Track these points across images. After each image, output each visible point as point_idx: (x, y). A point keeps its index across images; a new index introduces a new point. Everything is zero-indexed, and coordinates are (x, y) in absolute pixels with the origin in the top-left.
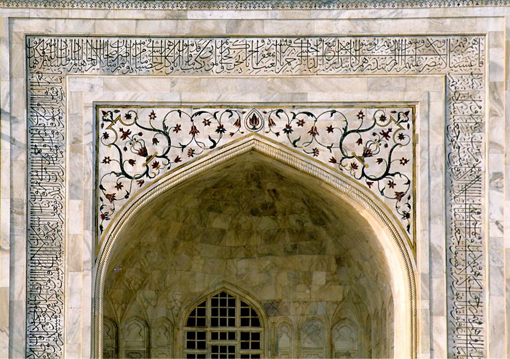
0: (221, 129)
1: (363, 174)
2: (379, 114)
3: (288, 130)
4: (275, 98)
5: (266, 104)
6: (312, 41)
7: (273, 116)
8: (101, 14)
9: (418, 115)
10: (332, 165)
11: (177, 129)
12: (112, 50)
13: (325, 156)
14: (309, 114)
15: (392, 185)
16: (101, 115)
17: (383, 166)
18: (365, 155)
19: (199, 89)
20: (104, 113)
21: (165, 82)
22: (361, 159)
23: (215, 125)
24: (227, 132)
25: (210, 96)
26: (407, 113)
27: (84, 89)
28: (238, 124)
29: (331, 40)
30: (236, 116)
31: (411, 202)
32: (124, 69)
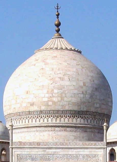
6: (69, 155)
32: (35, 160)
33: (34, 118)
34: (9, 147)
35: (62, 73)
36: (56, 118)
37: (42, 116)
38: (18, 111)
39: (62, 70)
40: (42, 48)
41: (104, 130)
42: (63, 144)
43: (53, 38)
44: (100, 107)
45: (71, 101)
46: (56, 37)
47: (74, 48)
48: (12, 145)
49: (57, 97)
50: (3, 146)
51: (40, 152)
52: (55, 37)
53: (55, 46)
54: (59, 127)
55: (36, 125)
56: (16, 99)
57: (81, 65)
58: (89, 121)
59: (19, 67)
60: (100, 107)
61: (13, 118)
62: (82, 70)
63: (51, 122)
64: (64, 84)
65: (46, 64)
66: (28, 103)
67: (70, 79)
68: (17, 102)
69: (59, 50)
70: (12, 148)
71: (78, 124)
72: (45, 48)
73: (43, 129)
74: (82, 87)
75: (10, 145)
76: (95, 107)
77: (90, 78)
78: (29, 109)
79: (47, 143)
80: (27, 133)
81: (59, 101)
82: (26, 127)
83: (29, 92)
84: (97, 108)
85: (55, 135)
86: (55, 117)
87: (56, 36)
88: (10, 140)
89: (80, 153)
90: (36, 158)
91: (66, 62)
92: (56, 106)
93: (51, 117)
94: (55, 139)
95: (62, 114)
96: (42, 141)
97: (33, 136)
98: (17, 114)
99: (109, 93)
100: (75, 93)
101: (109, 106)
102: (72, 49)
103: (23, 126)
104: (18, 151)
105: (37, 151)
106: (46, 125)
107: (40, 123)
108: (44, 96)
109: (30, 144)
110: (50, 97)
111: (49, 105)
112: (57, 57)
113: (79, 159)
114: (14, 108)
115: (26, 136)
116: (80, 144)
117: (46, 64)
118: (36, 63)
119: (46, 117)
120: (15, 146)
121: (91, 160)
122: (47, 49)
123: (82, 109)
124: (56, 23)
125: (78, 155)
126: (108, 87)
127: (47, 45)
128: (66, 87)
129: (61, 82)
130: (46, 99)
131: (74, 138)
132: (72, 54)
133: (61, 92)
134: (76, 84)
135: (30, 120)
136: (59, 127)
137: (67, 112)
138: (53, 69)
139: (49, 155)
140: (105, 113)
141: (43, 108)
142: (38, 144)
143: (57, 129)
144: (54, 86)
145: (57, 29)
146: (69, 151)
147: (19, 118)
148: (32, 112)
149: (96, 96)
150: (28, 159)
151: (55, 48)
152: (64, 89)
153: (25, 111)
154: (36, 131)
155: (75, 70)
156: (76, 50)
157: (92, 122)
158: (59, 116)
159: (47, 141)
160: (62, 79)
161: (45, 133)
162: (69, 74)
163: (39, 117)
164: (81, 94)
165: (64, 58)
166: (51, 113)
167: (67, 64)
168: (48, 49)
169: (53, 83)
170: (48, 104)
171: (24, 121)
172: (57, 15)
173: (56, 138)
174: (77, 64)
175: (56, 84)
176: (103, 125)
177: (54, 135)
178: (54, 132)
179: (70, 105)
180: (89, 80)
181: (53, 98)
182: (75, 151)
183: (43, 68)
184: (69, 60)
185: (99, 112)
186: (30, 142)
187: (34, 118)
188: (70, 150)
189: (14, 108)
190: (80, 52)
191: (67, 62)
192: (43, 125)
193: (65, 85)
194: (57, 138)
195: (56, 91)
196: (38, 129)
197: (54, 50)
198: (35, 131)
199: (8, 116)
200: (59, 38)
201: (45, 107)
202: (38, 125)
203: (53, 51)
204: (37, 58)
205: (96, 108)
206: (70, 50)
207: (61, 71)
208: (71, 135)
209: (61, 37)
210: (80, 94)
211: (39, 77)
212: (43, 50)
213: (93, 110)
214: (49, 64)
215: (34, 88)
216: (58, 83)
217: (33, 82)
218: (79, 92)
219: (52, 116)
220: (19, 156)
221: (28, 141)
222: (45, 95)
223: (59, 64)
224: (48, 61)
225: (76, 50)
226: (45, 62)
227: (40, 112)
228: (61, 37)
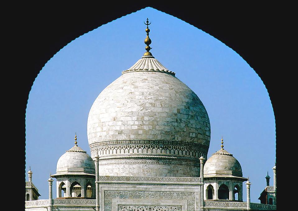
2: (175, 208)
4: (154, 204)
5: (152, 205)
6: (162, 192)
8: (119, 186)
9: (182, 208)
12: (122, 194)
14: (161, 207)
16: (119, 207)
19: (139, 201)
20: (120, 207)
21: (132, 200)
25: (142, 204)
26: (180, 208)
27: (116, 201)
28: (147, 209)
29: (165, 192)
33: (122, 148)
34: (95, 182)
35: (153, 98)
36: (147, 149)
37: (132, 146)
38: (104, 140)
39: (154, 95)
40: (130, 69)
41: (201, 164)
42: (155, 180)
43: (142, 58)
44: (197, 137)
46: (147, 56)
47: (167, 70)
48: (99, 179)
49: (148, 125)
50: (88, 180)
51: (130, 188)
52: (145, 56)
53: (146, 67)
54: (151, 159)
55: (125, 157)
56: (102, 126)
58: (184, 152)
60: (197, 137)
61: (99, 148)
62: (176, 95)
63: (141, 153)
64: (156, 111)
65: (136, 87)
66: (116, 131)
67: (162, 104)
68: (103, 130)
69: (150, 71)
70: (99, 183)
71: (171, 156)
72: (133, 69)
73: (133, 161)
74: (176, 115)
75: (96, 180)
77: (185, 104)
78: (116, 138)
79: (137, 179)
80: (115, 165)
81: (151, 130)
82: (114, 159)
83: (117, 119)
84: (194, 138)
85: (147, 168)
86: (146, 148)
87: (146, 55)
88: (96, 174)
89: (174, 190)
90: (125, 194)
91: (158, 86)
92: (147, 135)
94: (146, 172)
95: (154, 145)
96: (132, 176)
97: (122, 168)
98: (103, 144)
99: (207, 122)
100: (167, 121)
101: (207, 135)
102: (165, 71)
103: (110, 157)
104: (105, 187)
105: (127, 187)
106: (136, 156)
107: (129, 154)
108: (133, 124)
109: (119, 178)
110: (140, 125)
111: (139, 134)
112: (147, 80)
113: (173, 197)
114: (100, 136)
115: (114, 169)
116: (173, 179)
117: (135, 88)
118: (124, 86)
119: (135, 147)
120: (102, 181)
121: (186, 198)
122: (136, 70)
124: (146, 40)
125: (172, 192)
126: (206, 114)
127: (136, 66)
128: (158, 114)
129: (152, 108)
130: (136, 127)
131: (167, 172)
132: (165, 76)
133: (152, 120)
134: (169, 111)
135: (118, 151)
136: (150, 159)
138: (143, 94)
139: (139, 191)
140: (203, 144)
141: (132, 137)
142: (128, 178)
143: (148, 161)
145: (147, 47)
146: (162, 187)
147: (106, 148)
148: (120, 141)
149: (192, 125)
150: (117, 196)
151: (145, 70)
152: (156, 117)
153: (112, 140)
154: (125, 163)
155: (167, 94)
156: (169, 72)
157: (188, 154)
158: (150, 146)
159: (137, 175)
160: (153, 104)
161: (135, 165)
162: (161, 100)
163: (129, 147)
164: (175, 122)
165: (156, 81)
166: (141, 143)
167: (159, 88)
168: (137, 71)
169: (143, 109)
170: (138, 133)
171: (111, 151)
172: (146, 32)
173: (147, 171)
174: (170, 88)
175: (146, 110)
176: (199, 159)
177: (145, 168)
178: (145, 165)
179: (163, 135)
180: (183, 106)
181: (143, 126)
182: (168, 187)
184: (161, 84)
185: (195, 143)
186: (119, 176)
187: (122, 148)
188: (164, 187)
189: (100, 136)
190: (173, 74)
191: (159, 85)
192: (133, 156)
193: (156, 112)
194: (148, 171)
195: (146, 118)
196: (128, 161)
197: (143, 72)
198: (124, 163)
200: (149, 58)
201: (134, 135)
202: (127, 157)
203: (143, 73)
205: (192, 138)
206: (162, 72)
208: (164, 169)
209: (152, 56)
211: (128, 102)
212: (131, 71)
213: (188, 140)
215: (121, 114)
216: (149, 110)
218: (172, 120)
219: (142, 147)
220: (107, 192)
221: (116, 175)
222: (134, 123)
223: (149, 88)
224: (137, 84)
225: (169, 72)
226: (134, 85)
227: (129, 141)
228: (152, 56)
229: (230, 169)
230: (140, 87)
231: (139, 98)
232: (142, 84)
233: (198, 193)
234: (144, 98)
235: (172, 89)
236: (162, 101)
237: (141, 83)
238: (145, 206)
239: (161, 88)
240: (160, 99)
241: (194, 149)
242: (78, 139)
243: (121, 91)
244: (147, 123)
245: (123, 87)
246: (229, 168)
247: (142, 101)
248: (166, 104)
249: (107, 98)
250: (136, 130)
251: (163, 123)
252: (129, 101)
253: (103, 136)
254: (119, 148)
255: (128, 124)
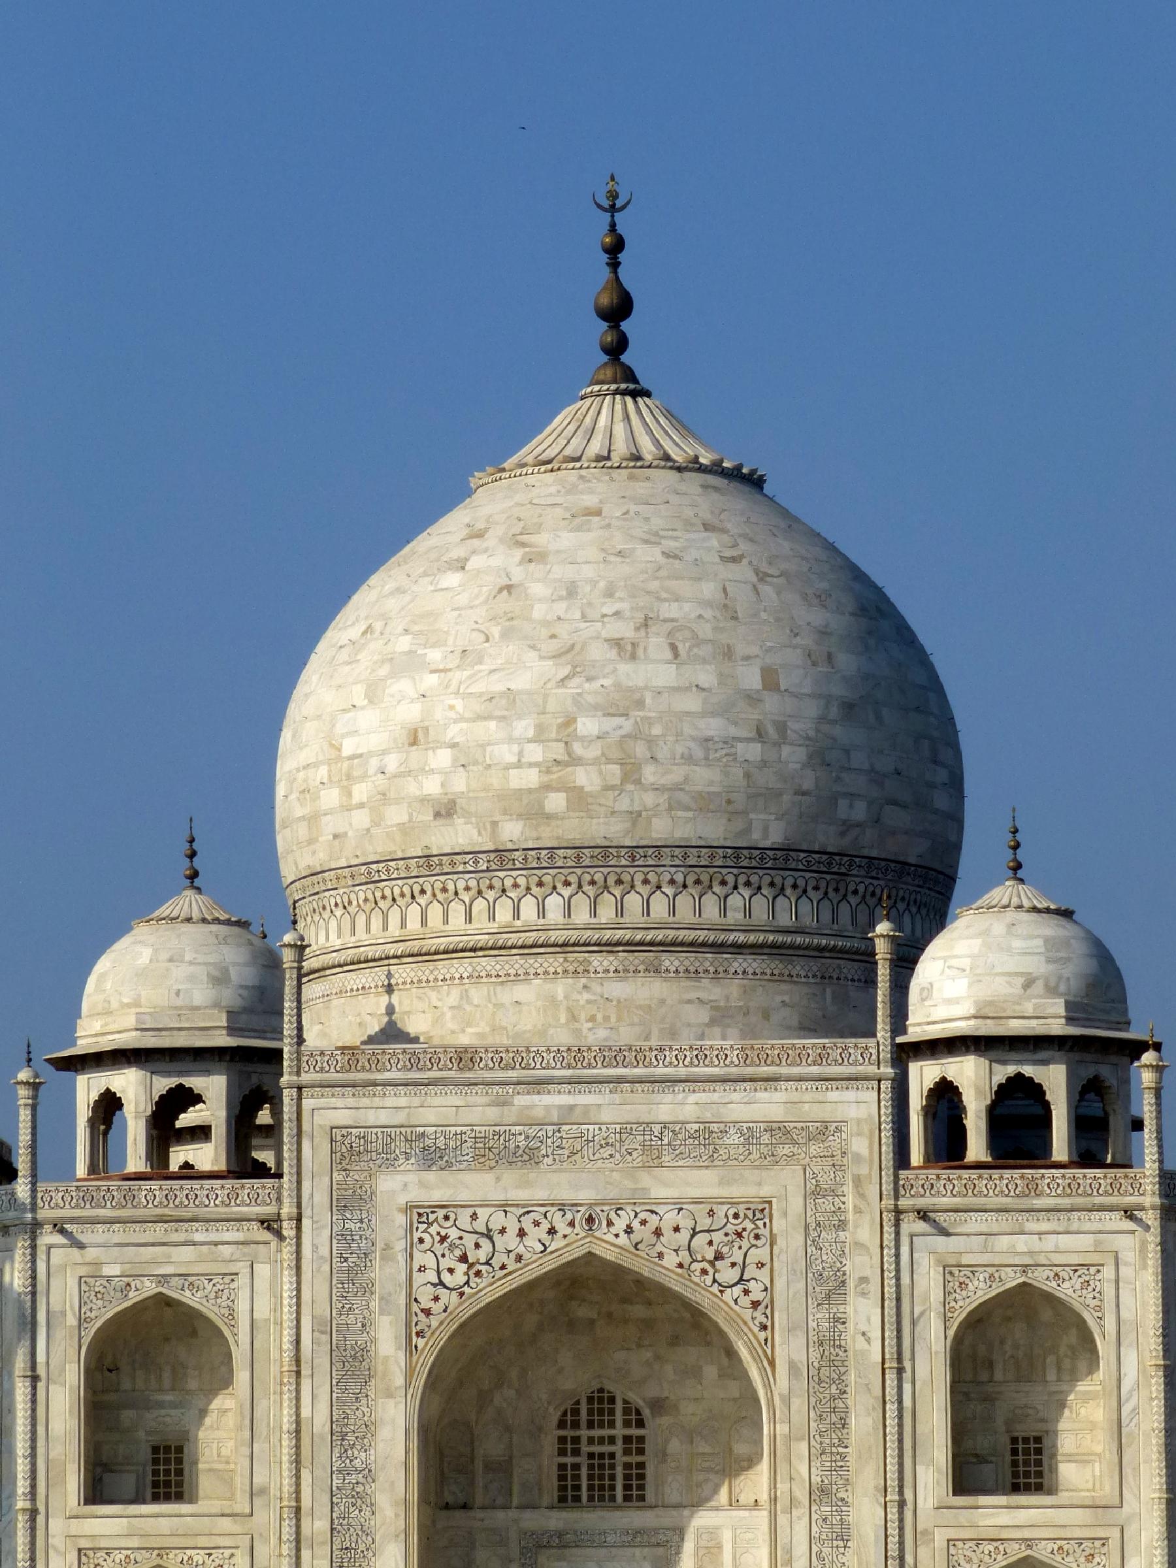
0: (552, 1231)
1: (715, 1281)
3: (629, 1230)
7: (613, 1215)
10: (679, 1270)
11: (503, 1231)
13: (671, 1260)
15: (746, 1292)
17: (738, 1269)
18: (716, 1259)
20: (420, 1215)
22: (712, 1263)
23: (545, 1226)
24: (560, 1235)
28: (572, 1224)
30: (569, 1216)
31: (768, 1312)
35: (628, 614)
45: (687, 788)
49: (595, 762)
57: (750, 563)
59: (374, 580)
66: (424, 800)
67: (680, 646)
68: (356, 799)
76: (844, 822)
81: (612, 788)
93: (559, 885)
101: (936, 812)
112: (598, 513)
117: (530, 561)
118: (474, 552)
123: (756, 838)
136: (610, 946)
137: (659, 856)
138: (572, 591)
144: (579, 694)
148: (444, 858)
152: (641, 714)
153: (400, 855)
155: (709, 589)
162: (673, 620)
165: (647, 519)
171: (394, 917)
174: (728, 553)
183: (515, 581)
193: (646, 688)
195: (587, 726)
199: (304, 889)
203: (581, 477)
204: (481, 525)
207: (621, 599)
210: (740, 740)
214: (551, 558)
217: (450, 670)
218: (733, 731)
224: (541, 539)
226: (524, 545)
229: (1052, 991)
230: (558, 552)
231: (549, 618)
232: (567, 540)
233: (866, 1129)
234: (578, 615)
235: (733, 560)
236: (679, 629)
237: (565, 535)
238: (562, 1208)
239: (676, 557)
240: (667, 616)
241: (861, 888)
242: (213, 842)
243: (452, 579)
244: (593, 752)
245: (467, 560)
246: (1052, 984)
247: (562, 630)
248: (697, 641)
249: (378, 626)
250: (530, 791)
251: (680, 749)
252: (495, 631)
253: (350, 834)
254: (440, 896)
255: (488, 762)
